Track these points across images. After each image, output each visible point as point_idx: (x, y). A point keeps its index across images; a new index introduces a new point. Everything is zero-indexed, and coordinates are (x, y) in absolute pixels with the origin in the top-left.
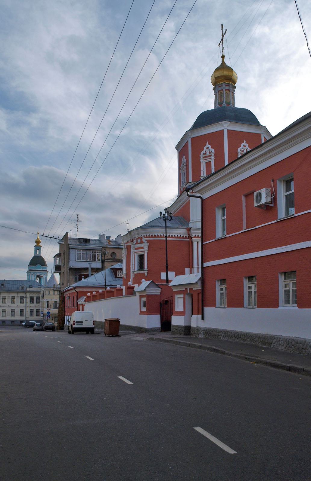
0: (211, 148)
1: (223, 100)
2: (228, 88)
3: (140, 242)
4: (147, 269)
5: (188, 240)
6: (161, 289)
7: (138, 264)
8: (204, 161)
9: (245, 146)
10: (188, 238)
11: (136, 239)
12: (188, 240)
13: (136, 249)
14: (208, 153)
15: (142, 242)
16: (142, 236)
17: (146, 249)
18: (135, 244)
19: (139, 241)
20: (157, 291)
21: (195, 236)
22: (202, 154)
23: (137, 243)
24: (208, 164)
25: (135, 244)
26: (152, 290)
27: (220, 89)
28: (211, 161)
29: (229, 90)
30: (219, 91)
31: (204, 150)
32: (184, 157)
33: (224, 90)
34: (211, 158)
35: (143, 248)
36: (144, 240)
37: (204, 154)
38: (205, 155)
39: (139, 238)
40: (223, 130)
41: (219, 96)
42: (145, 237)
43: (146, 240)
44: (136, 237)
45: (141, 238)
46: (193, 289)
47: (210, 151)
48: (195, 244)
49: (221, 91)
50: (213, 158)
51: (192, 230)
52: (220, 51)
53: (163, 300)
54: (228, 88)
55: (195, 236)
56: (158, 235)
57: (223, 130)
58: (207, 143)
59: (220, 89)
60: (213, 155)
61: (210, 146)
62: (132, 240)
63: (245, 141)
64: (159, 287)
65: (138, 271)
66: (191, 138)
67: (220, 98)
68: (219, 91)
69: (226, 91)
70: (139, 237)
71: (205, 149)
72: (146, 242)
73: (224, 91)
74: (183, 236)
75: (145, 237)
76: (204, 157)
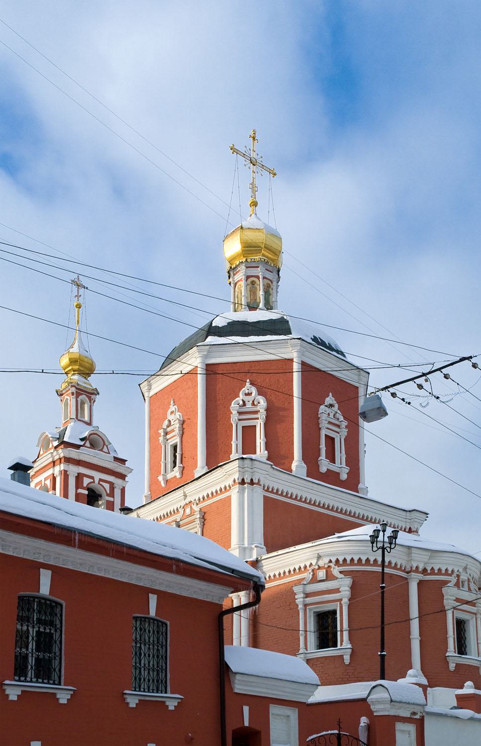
14: (249, 405)
24: (249, 433)
28: (255, 426)
38: (244, 409)
50: (262, 415)
61: (254, 390)
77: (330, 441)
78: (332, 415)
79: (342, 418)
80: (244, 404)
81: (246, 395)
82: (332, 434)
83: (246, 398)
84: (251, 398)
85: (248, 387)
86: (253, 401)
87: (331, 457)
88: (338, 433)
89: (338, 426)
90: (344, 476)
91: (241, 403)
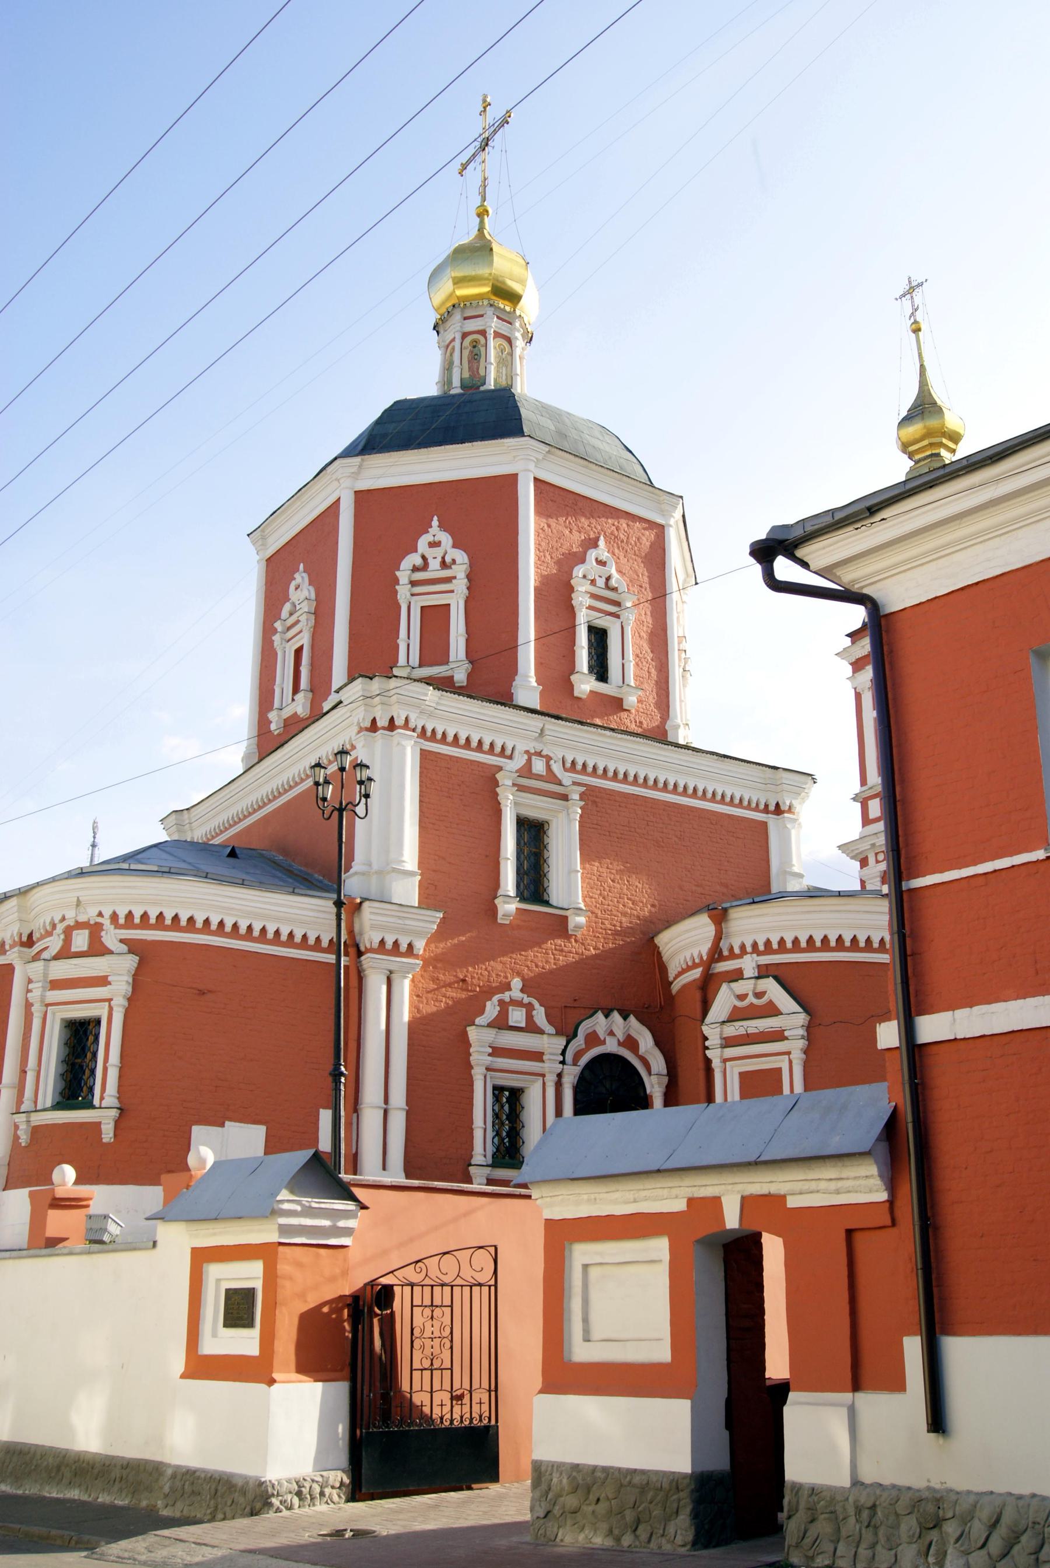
0: (454, 546)
1: (482, 372)
2: (504, 328)
3: (85, 948)
4: (114, 1102)
7: (61, 1070)
9: (601, 563)
11: (60, 928)
13: (57, 985)
14: (434, 564)
15: (96, 949)
16: (100, 914)
17: (120, 988)
18: (56, 958)
19: (81, 941)
21: (382, 942)
23: (65, 954)
25: (56, 958)
30: (465, 335)
31: (416, 551)
32: (301, 578)
35: (102, 981)
36: (111, 937)
37: (415, 569)
38: (419, 576)
39: (79, 925)
40: (514, 477)
41: (466, 353)
42: (122, 921)
43: (122, 941)
44: (63, 919)
45: (95, 930)
46: (792, 1202)
47: (448, 559)
51: (369, 914)
54: (504, 328)
55: (382, 942)
56: (191, 920)
57: (514, 477)
58: (435, 522)
59: (472, 325)
61: (446, 539)
62: (30, 936)
63: (602, 543)
65: (58, 1106)
66: (355, 492)
67: (469, 362)
68: (465, 335)
70: (82, 918)
71: (422, 543)
72: (124, 948)
75: (122, 921)
76: (413, 583)
78: (601, 582)
80: (425, 567)
82: (602, 622)
83: (430, 553)
84: (438, 552)
85: (435, 532)
86: (443, 558)
87: (600, 669)
88: (618, 617)
89: (617, 604)
91: (419, 562)
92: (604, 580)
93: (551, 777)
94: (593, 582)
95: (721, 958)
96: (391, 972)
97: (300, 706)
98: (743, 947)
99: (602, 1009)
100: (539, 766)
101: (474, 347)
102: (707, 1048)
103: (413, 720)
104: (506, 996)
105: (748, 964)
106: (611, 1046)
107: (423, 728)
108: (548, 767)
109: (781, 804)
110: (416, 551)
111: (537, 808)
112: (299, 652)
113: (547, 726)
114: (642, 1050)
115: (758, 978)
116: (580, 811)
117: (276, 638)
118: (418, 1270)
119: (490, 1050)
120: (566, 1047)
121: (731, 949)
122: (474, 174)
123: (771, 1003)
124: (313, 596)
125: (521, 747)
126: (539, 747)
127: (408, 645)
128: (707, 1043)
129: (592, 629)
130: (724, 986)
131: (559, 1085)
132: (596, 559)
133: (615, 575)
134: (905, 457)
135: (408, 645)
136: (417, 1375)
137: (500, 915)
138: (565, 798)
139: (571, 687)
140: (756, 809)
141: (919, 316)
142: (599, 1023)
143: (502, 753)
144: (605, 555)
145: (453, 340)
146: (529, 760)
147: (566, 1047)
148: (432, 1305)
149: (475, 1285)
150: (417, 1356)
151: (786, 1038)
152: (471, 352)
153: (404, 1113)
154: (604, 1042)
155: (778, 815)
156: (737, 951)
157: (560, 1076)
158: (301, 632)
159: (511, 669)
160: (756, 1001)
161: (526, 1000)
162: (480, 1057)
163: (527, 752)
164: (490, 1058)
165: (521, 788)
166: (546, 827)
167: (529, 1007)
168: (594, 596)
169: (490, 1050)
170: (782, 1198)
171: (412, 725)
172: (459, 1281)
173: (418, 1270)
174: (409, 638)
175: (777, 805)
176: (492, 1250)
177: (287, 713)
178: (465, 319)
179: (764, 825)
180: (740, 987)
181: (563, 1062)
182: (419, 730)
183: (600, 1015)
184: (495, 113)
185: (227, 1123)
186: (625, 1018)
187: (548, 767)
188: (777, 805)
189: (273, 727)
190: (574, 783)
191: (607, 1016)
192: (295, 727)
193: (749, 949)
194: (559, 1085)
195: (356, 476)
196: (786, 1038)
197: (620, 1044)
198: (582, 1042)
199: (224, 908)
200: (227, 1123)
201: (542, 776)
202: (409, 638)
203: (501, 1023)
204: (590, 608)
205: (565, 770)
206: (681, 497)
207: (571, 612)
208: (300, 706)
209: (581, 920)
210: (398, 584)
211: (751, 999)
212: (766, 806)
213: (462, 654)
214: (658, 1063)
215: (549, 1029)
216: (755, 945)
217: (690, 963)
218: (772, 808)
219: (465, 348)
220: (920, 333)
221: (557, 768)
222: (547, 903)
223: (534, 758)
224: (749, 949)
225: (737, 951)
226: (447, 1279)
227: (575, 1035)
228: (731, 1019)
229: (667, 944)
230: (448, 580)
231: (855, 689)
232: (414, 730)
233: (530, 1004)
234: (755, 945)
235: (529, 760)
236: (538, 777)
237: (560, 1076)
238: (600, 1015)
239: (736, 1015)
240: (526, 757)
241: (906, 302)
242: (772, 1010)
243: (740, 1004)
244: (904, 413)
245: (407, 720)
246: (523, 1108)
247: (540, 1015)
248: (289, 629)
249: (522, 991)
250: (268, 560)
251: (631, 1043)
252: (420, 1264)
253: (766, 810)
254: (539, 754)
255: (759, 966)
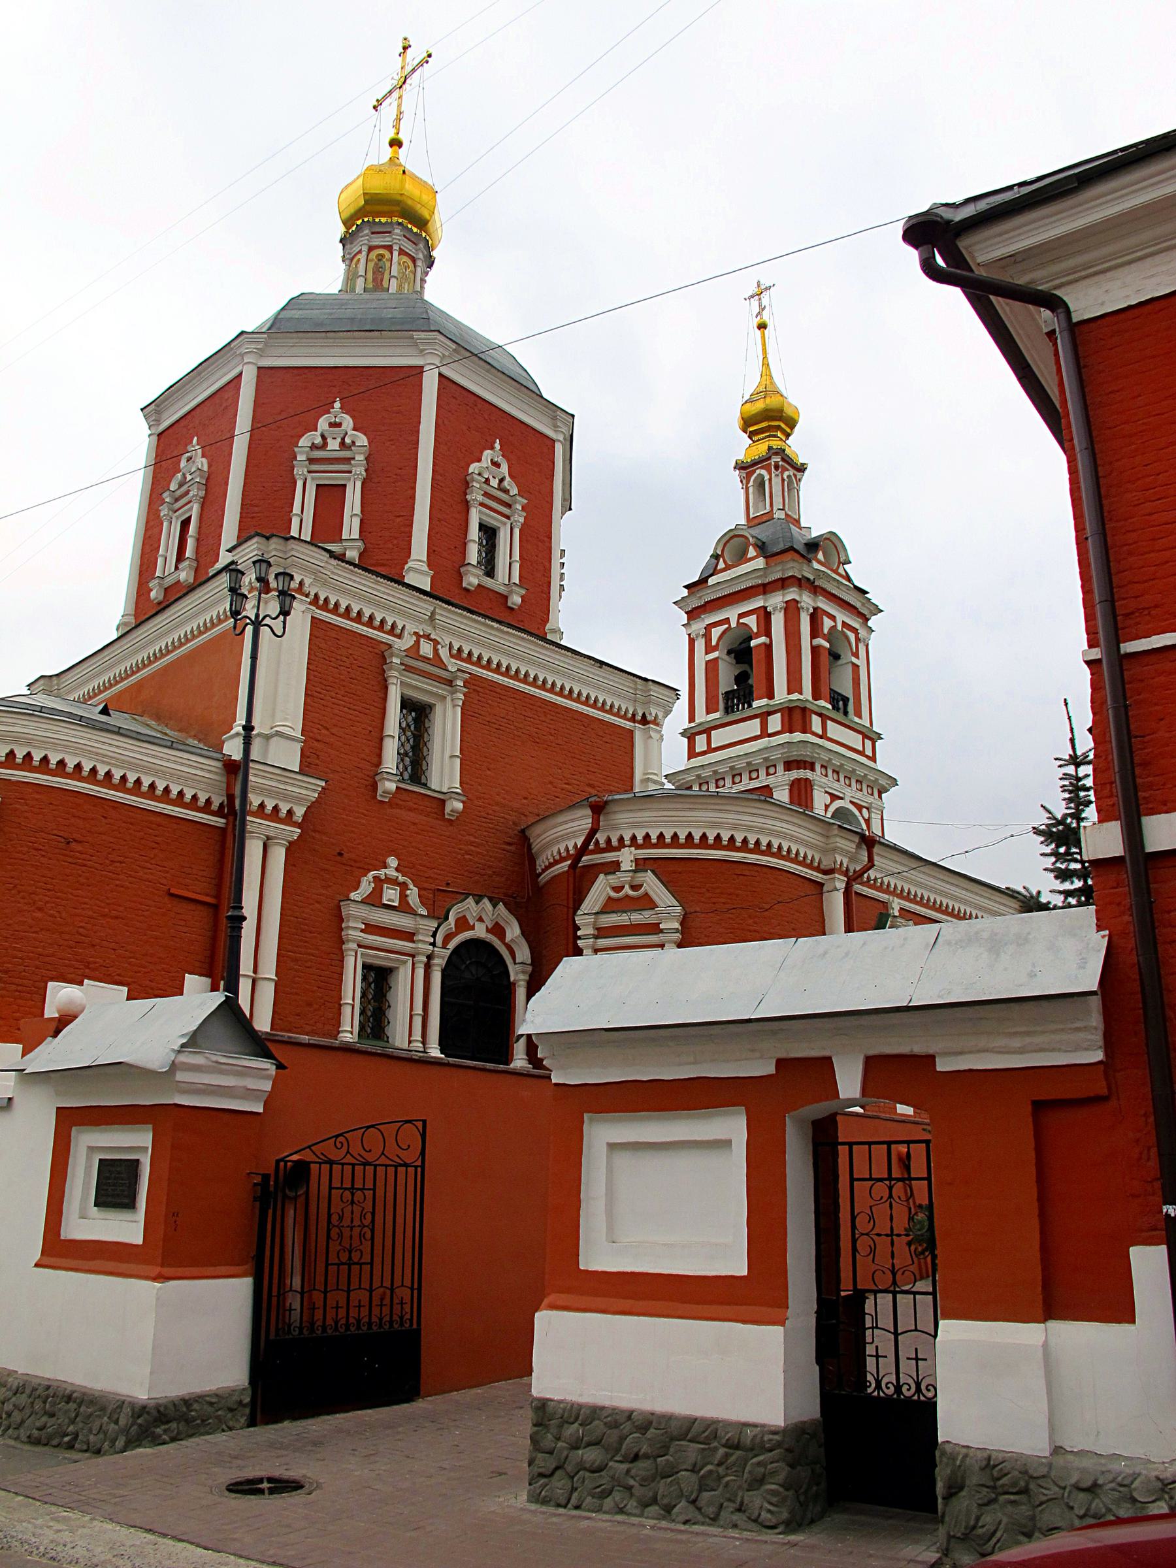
0: (354, 429)
2: (409, 247)
5: (219, 821)
6: (280, 1066)
8: (309, 476)
9: (496, 464)
10: (219, 813)
12: (219, 821)
14: (333, 445)
20: (251, 1083)
22: (304, 442)
26: (217, 1069)
27: (377, 241)
28: (345, 486)
29: (414, 260)
31: (316, 430)
33: (396, 247)
34: (350, 472)
37: (314, 447)
40: (419, 370)
41: (371, 265)
46: (942, 1066)
47: (348, 441)
48: (253, 850)
49: (382, 251)
52: (377, 128)
53: (282, 1160)
54: (409, 247)
57: (419, 370)
58: (337, 405)
60: (360, 458)
61: (348, 422)
63: (497, 446)
64: (267, 1055)
66: (259, 368)
67: (374, 273)
68: (371, 249)
69: (405, 258)
71: (323, 424)
73: (395, 254)
74: (195, 798)
76: (312, 461)
77: (489, 533)
78: (494, 483)
79: (514, 491)
80: (325, 444)
81: (332, 425)
82: (493, 520)
86: (343, 439)
88: (508, 518)
89: (509, 506)
90: (516, 600)
91: (318, 440)
92: (497, 481)
93: (437, 661)
94: (487, 481)
95: (599, 850)
96: (268, 838)
97: (185, 575)
98: (621, 839)
99: (474, 895)
100: (426, 649)
101: (380, 260)
102: (579, 938)
103: (307, 585)
104: (382, 873)
105: (626, 858)
106: (480, 932)
107: (316, 595)
108: (436, 651)
109: (647, 715)
110: (316, 430)
111: (423, 689)
112: (186, 524)
113: (437, 611)
114: (509, 937)
115: (635, 871)
116: (462, 697)
117: (164, 511)
118: (339, 1146)
119: (363, 927)
120: (437, 929)
121: (609, 841)
122: (389, 110)
123: (647, 894)
124: (205, 468)
125: (411, 628)
126: (429, 630)
127: (301, 521)
128: (579, 933)
129: (483, 527)
130: (602, 876)
131: (428, 967)
132: (492, 460)
133: (508, 479)
134: (745, 436)
135: (301, 521)
136: (332, 1269)
137: (379, 792)
138: (450, 683)
139: (460, 577)
140: (624, 717)
141: (766, 316)
142: (469, 907)
143: (392, 631)
144: (499, 459)
145: (360, 252)
146: (417, 643)
147: (437, 929)
148: (353, 1188)
149: (401, 1165)
150: (334, 1247)
151: (661, 931)
152: (376, 264)
153: (273, 985)
154: (473, 928)
155: (644, 725)
156: (615, 843)
157: (430, 957)
158: (190, 502)
159: (406, 552)
160: (631, 893)
161: (401, 879)
162: (353, 932)
163: (416, 633)
164: (362, 934)
165: (409, 669)
166: (428, 711)
167: (404, 886)
168: (486, 494)
169: (363, 926)
170: (931, 1059)
171: (306, 589)
172: (383, 1160)
173: (339, 1146)
174: (302, 513)
175: (644, 715)
176: (420, 1125)
177: (169, 581)
178: (373, 233)
179: (631, 732)
180: (613, 879)
181: (433, 944)
182: (312, 596)
183: (470, 900)
184: (415, 56)
185: (86, 981)
186: (494, 906)
187: (436, 651)
188: (644, 715)
189: (153, 594)
190: (459, 670)
191: (477, 903)
192: (175, 594)
193: (627, 842)
194: (428, 967)
195: (261, 353)
196: (661, 931)
197: (488, 930)
198: (453, 925)
199: (97, 754)
200: (86, 981)
201: (429, 659)
202: (302, 513)
203: (374, 900)
204: (482, 504)
205: (452, 656)
206: (573, 416)
207: (467, 506)
208: (185, 575)
209: (460, 806)
210: (296, 460)
211: (627, 890)
212: (634, 715)
213: (356, 535)
214: (524, 953)
215: (423, 911)
216: (634, 838)
217: (564, 855)
218: (639, 718)
219: (372, 260)
220: (766, 331)
221: (444, 653)
222: (425, 785)
223: (422, 640)
224: (627, 842)
225: (615, 843)
226: (370, 1158)
227: (446, 918)
228: (602, 912)
229: (539, 836)
230: (348, 460)
231: (689, 635)
232: (307, 596)
233: (404, 883)
234: (634, 838)
235: (417, 643)
236: (425, 659)
237: (430, 957)
238: (470, 900)
239: (611, 906)
240: (414, 638)
241: (755, 302)
242: (647, 902)
243: (613, 894)
244: (747, 397)
245: (301, 583)
246: (390, 988)
247: (413, 893)
248: (177, 500)
249: (397, 870)
250: (159, 435)
251: (498, 930)
252: (341, 1139)
253: (633, 719)
254: (427, 637)
255: (636, 860)
